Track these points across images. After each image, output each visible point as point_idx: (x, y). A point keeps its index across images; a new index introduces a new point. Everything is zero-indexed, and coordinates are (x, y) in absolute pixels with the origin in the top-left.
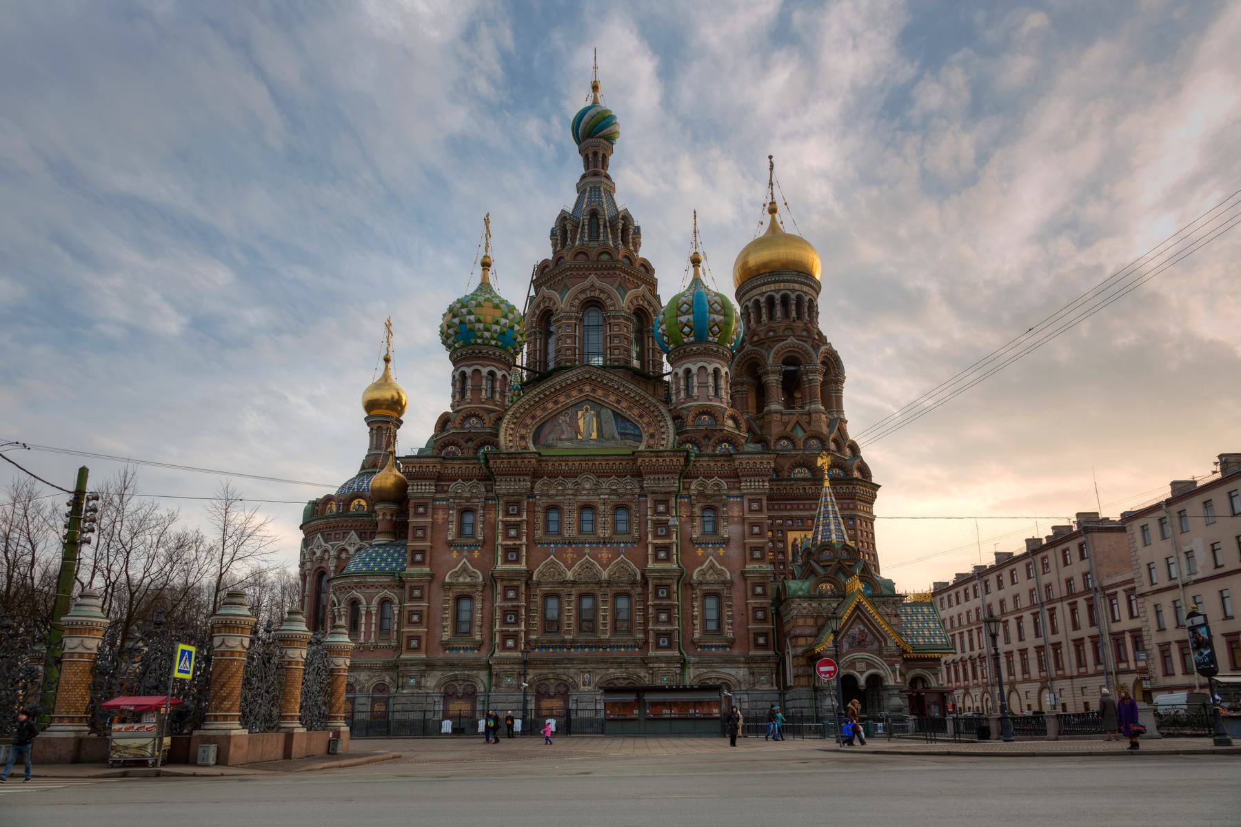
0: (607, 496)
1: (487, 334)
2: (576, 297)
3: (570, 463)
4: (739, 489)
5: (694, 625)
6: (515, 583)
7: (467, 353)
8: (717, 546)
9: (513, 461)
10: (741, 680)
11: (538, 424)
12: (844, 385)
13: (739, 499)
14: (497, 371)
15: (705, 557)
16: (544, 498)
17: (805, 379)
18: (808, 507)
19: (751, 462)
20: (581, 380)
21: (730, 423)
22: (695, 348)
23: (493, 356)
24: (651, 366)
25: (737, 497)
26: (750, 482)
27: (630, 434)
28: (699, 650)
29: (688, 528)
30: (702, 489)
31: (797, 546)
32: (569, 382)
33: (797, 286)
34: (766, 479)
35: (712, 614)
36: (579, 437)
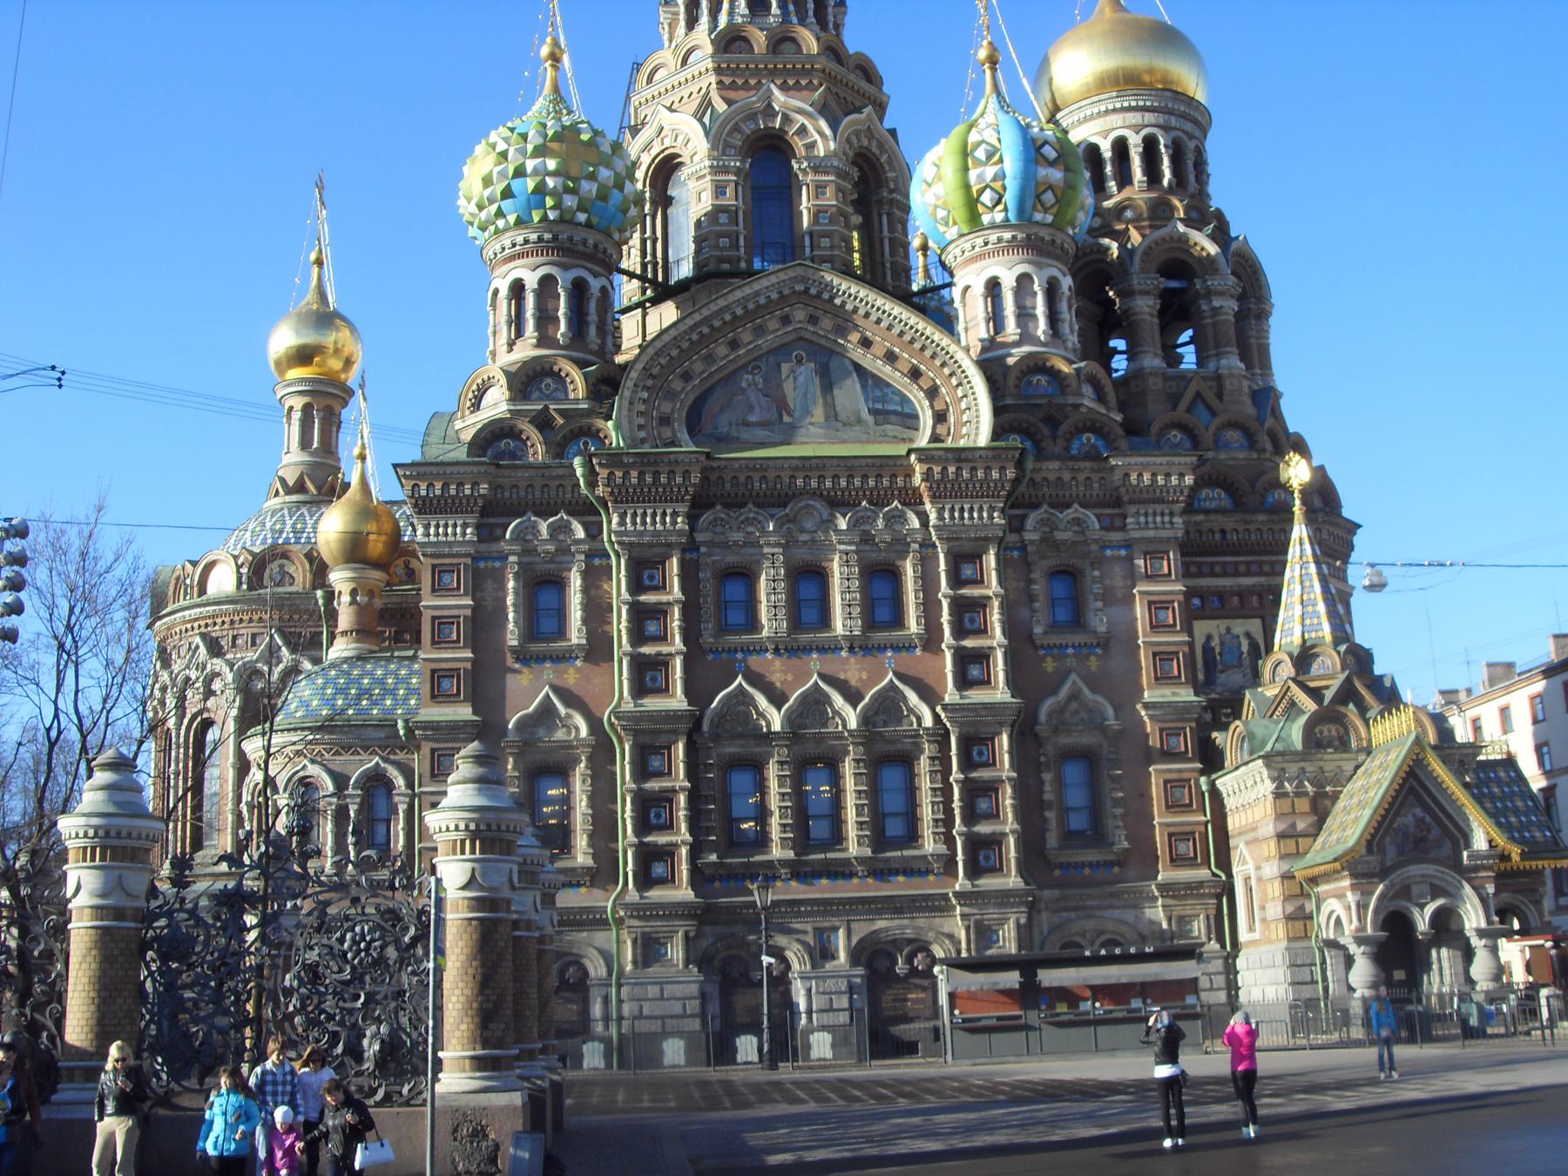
4: (1123, 528)
5: (1045, 820)
7: (526, 241)
8: (1085, 651)
10: (1146, 933)
11: (698, 392)
12: (1272, 320)
13: (1123, 552)
14: (590, 279)
16: (717, 550)
18: (1230, 569)
20: (782, 296)
21: (1087, 390)
23: (580, 248)
24: (889, 272)
25: (1119, 547)
26: (1146, 515)
27: (895, 413)
28: (1057, 873)
30: (1047, 529)
31: (1213, 649)
35: (1077, 797)
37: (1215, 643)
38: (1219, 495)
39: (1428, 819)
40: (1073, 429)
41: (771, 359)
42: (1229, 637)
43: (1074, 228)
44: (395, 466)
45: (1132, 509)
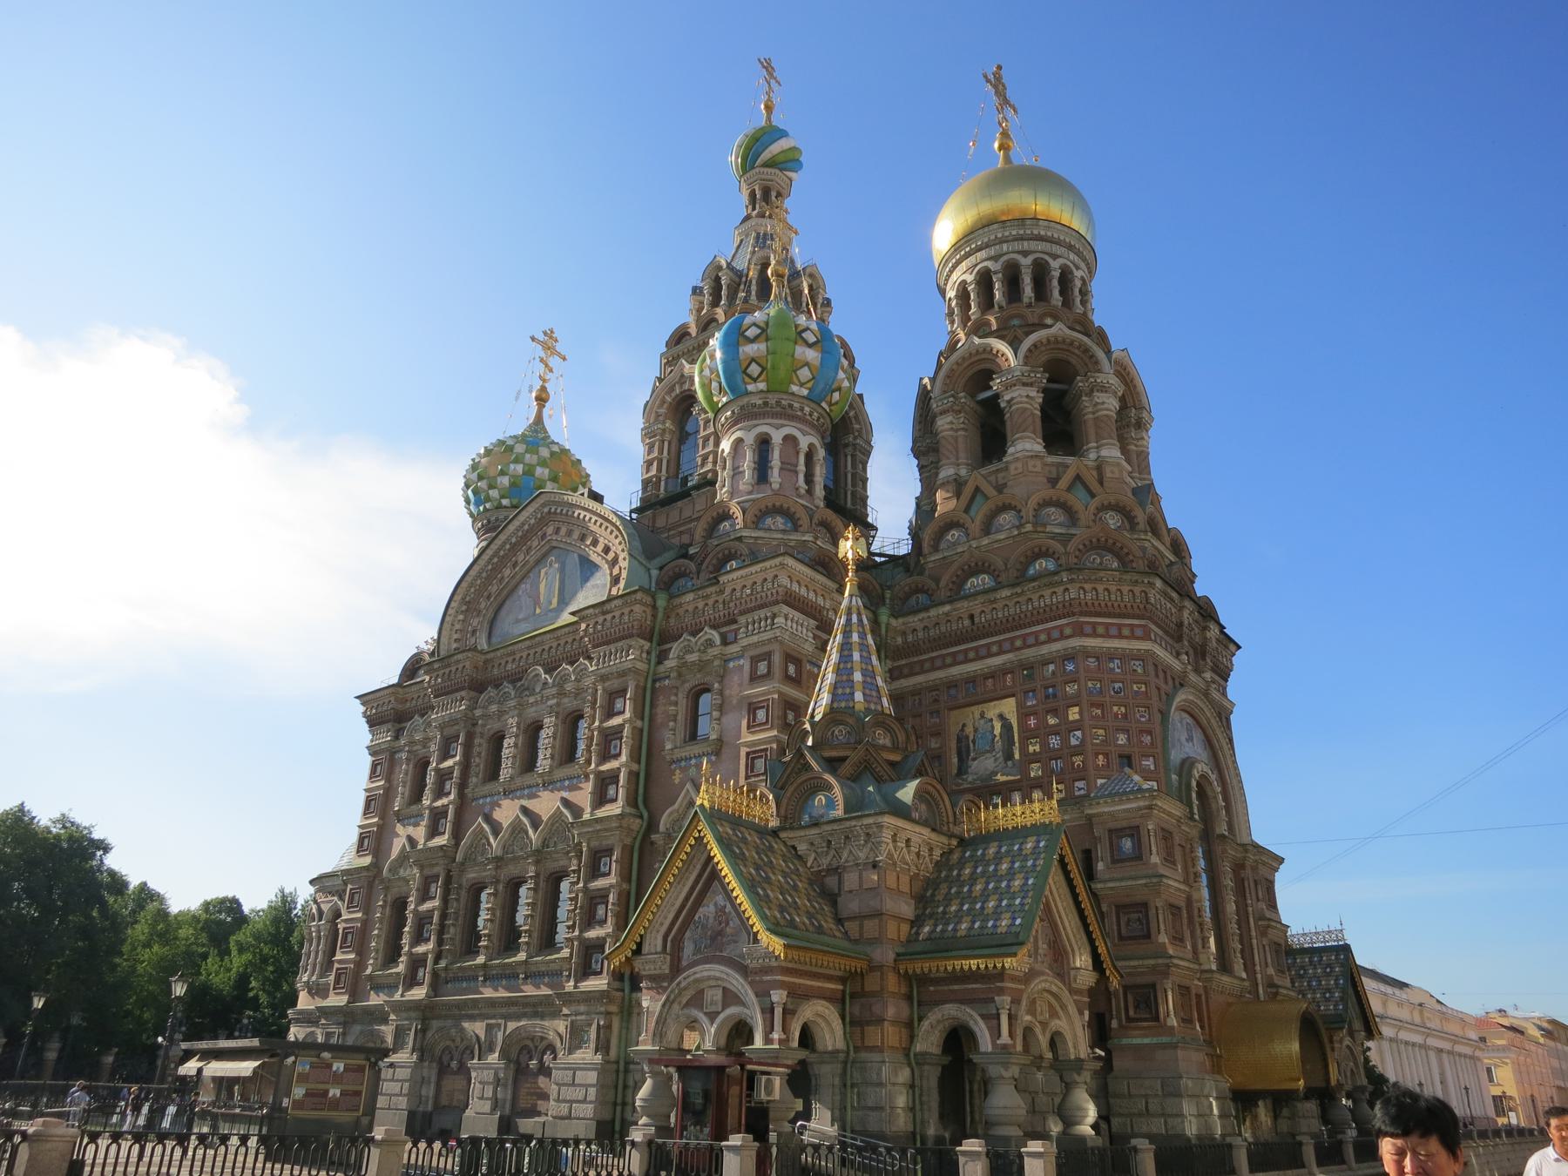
0: (555, 701)
1: (494, 493)
2: (663, 402)
3: (518, 656)
6: (436, 870)
9: (447, 671)
11: (495, 605)
13: (742, 662)
15: (682, 785)
16: (490, 721)
17: (1003, 405)
18: (983, 652)
19: (749, 583)
22: (729, 413)
25: (738, 658)
29: (668, 734)
31: (967, 737)
32: (526, 527)
33: (1005, 247)
34: (775, 609)
36: (538, 611)
37: (969, 730)
38: (983, 580)
39: (729, 908)
40: (714, 561)
41: (537, 569)
42: (982, 722)
43: (802, 385)
44: (357, 697)
45: (742, 620)
